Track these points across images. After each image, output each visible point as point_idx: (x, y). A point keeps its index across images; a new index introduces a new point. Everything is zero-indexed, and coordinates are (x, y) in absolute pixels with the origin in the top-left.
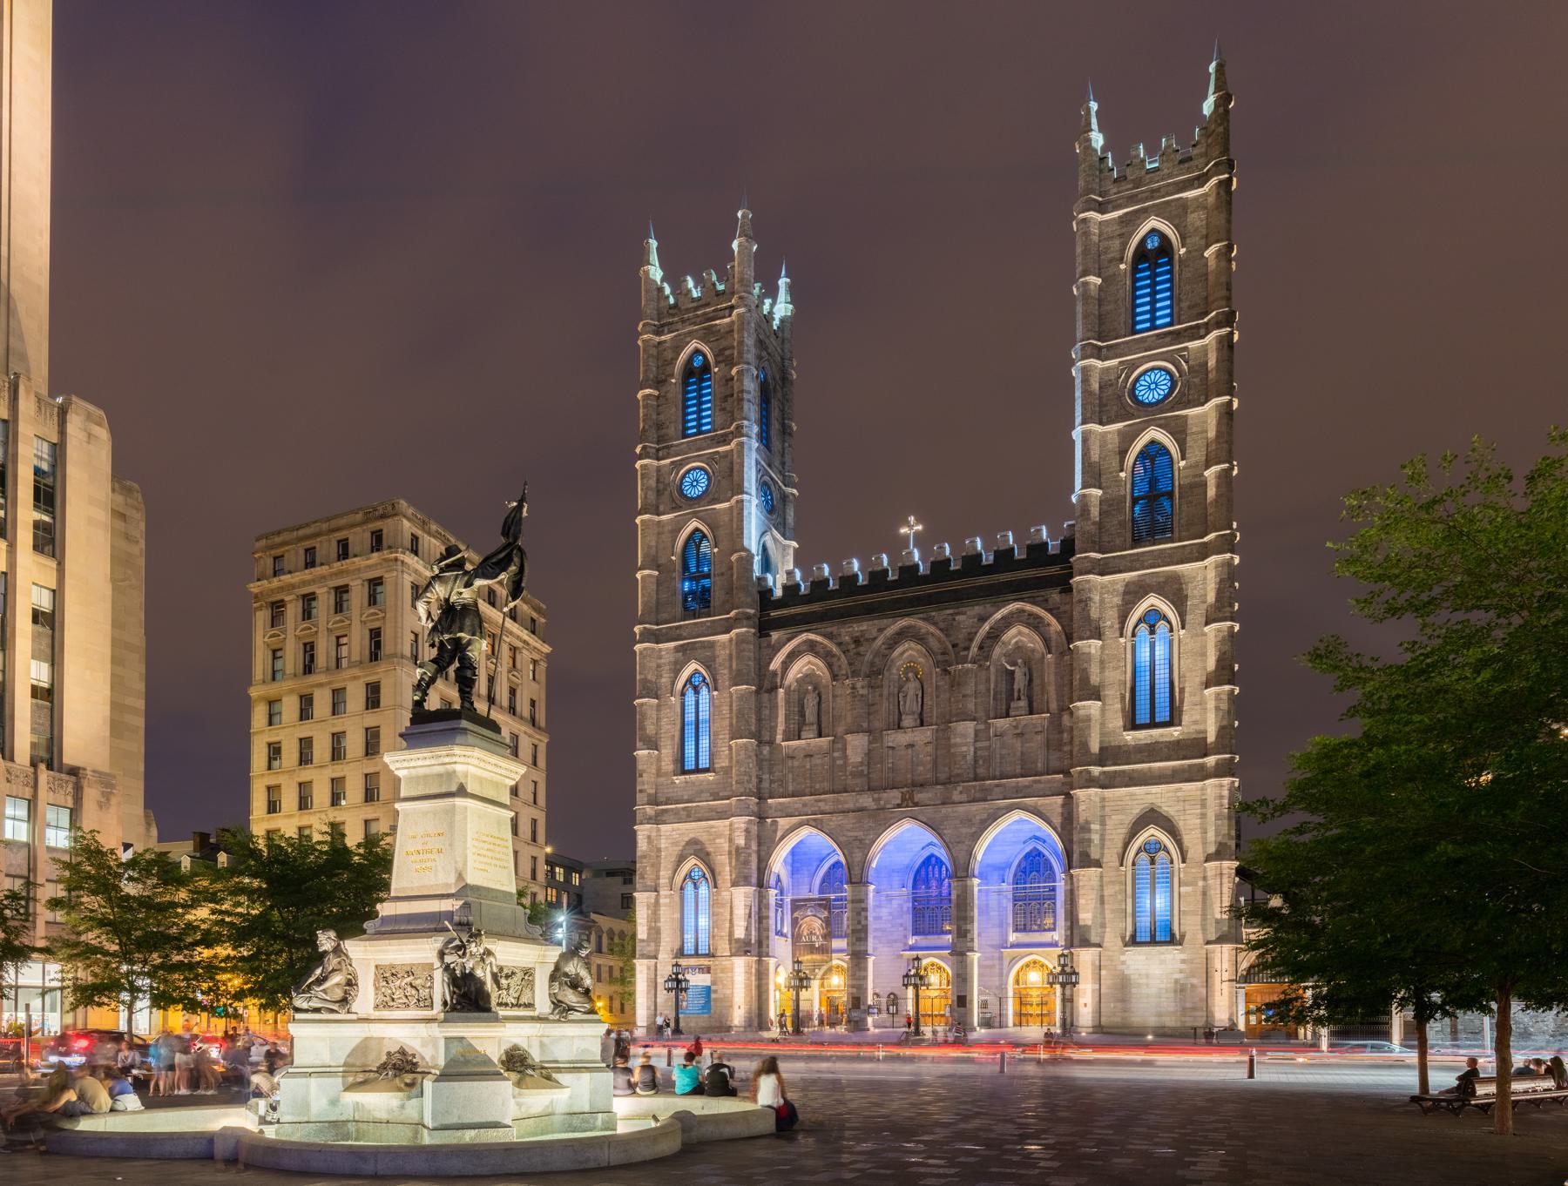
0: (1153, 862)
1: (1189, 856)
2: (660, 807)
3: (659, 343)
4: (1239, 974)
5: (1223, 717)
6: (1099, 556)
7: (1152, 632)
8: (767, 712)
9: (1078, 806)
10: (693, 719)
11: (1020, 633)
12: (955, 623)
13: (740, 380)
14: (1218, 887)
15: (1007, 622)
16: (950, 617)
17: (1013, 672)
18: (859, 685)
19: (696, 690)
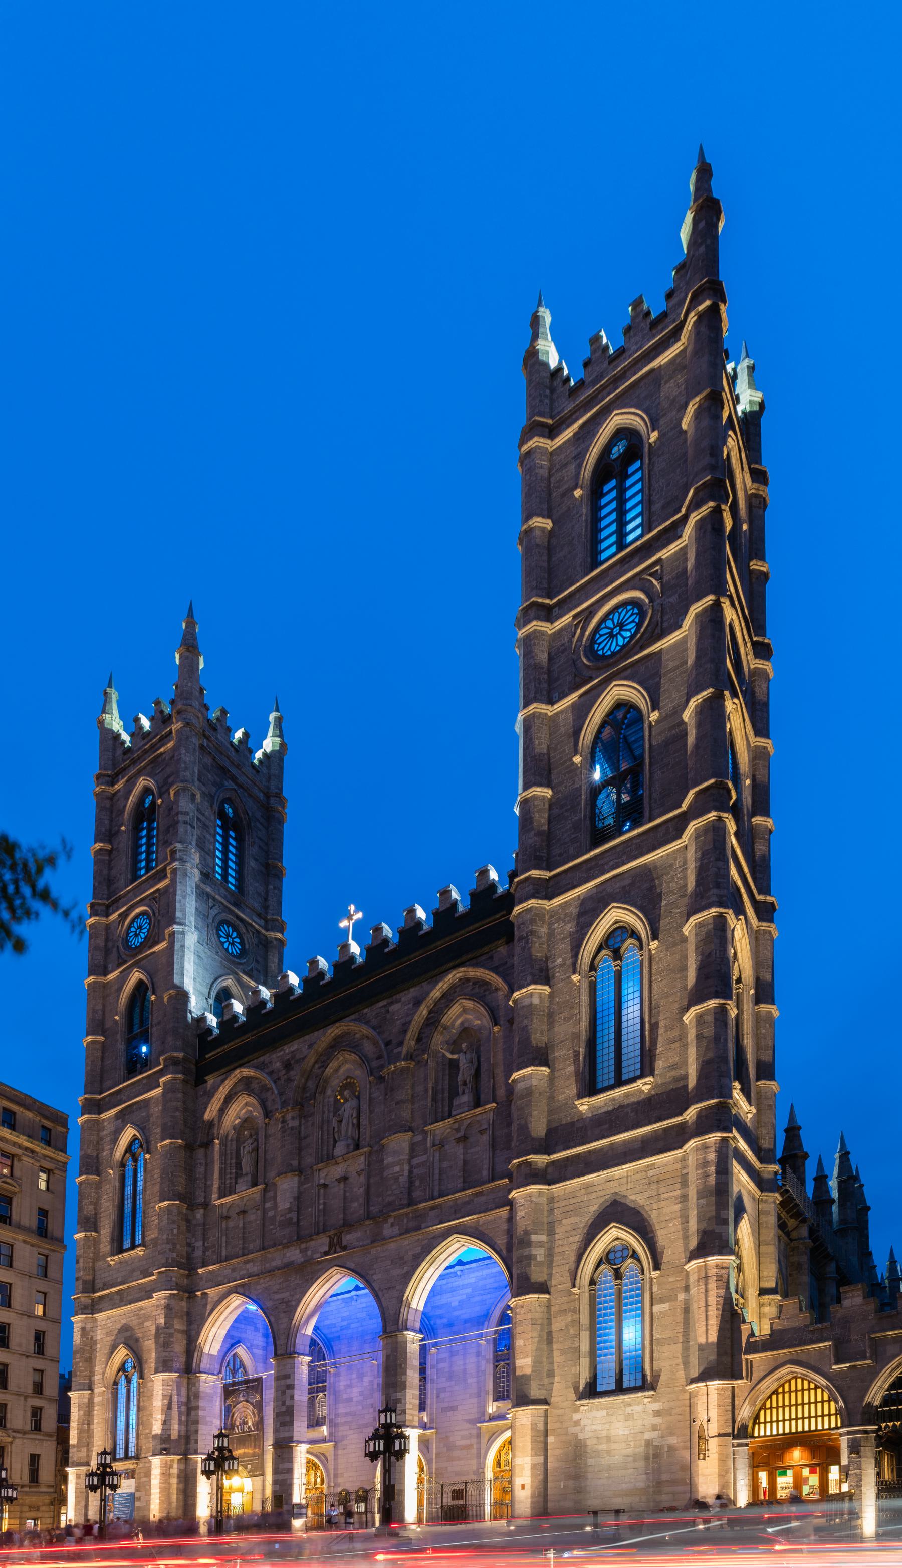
8: (202, 1169)
11: (465, 1010)
14: (703, 1296)
15: (448, 999)
16: (383, 1010)
17: (457, 1061)
18: (289, 1117)
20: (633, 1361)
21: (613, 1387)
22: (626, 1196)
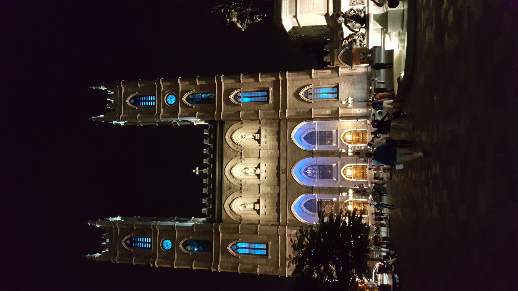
0: (311, 94)
1: (310, 83)
2: (280, 265)
4: (349, 67)
5: (268, 76)
9: (291, 116)
10: (248, 250)
12: (229, 156)
19: (239, 248)
20: (332, 90)
21: (337, 94)
22: (294, 92)
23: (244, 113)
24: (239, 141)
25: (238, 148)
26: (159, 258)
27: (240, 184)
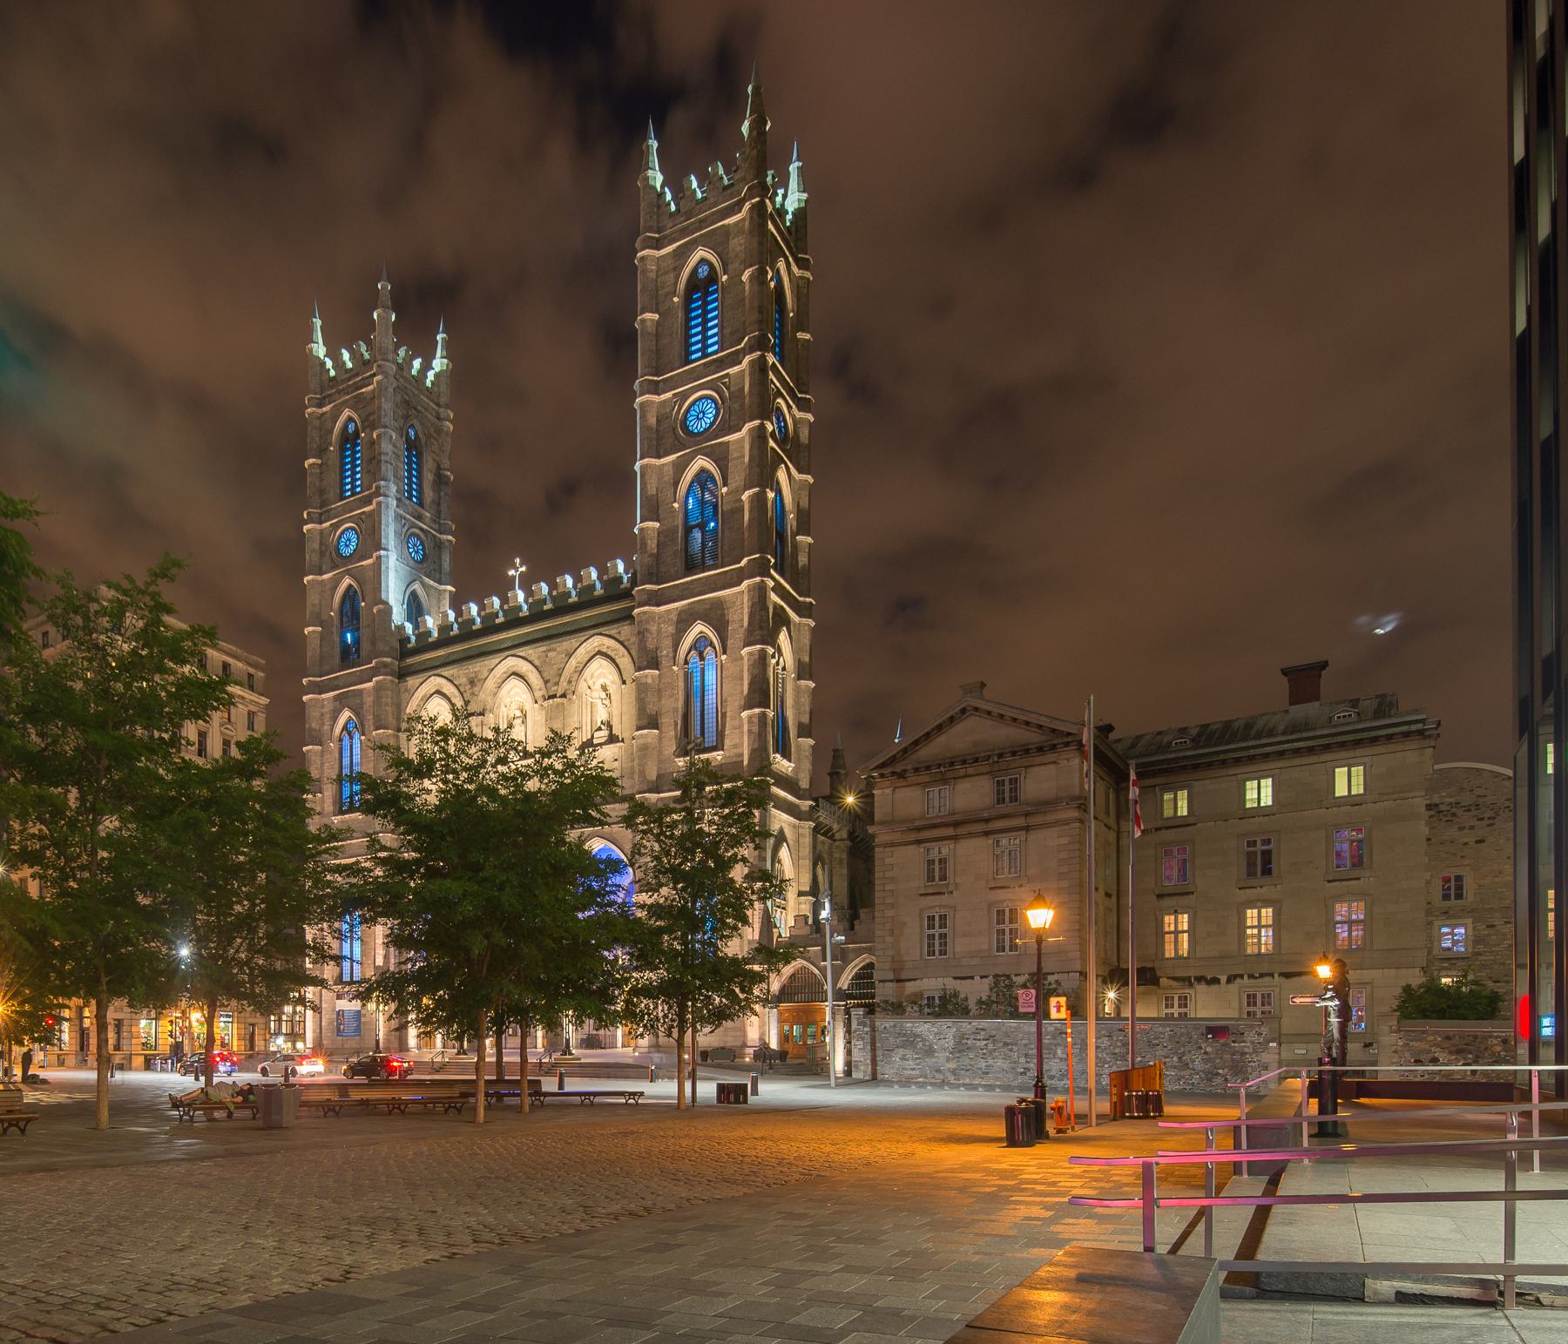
3: (322, 414)
6: (656, 587)
7: (702, 658)
13: (379, 444)
23: (650, 681)
24: (590, 683)
25: (570, 682)
26: (322, 531)
27: (484, 710)
